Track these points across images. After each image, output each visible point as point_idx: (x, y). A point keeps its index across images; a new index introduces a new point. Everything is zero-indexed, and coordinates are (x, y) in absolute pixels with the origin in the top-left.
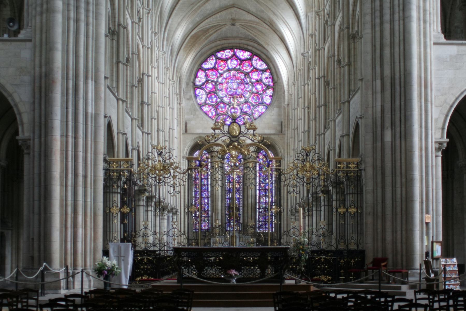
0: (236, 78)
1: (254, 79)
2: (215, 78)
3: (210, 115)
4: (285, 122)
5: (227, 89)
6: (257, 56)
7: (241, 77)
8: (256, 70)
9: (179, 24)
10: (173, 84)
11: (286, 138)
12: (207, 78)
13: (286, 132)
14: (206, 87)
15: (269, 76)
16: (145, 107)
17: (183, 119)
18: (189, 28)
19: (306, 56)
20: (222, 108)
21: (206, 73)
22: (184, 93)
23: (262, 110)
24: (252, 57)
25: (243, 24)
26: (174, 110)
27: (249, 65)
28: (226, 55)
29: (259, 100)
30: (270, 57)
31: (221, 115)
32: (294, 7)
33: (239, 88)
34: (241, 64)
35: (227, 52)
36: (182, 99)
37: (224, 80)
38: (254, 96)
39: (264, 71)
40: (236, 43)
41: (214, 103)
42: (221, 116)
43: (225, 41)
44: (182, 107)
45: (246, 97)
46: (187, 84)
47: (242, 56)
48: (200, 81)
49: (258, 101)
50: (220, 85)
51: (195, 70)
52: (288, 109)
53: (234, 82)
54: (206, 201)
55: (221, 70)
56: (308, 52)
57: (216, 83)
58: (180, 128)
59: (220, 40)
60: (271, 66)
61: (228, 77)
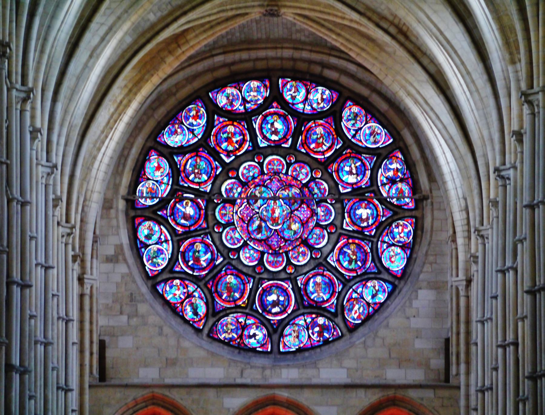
2: (206, 182)
3: (189, 315)
4: (458, 344)
5: (251, 221)
6: (356, 104)
7: (301, 177)
9: (94, 54)
10: (69, 235)
11: (462, 403)
12: (178, 184)
13: (462, 378)
15: (399, 174)
16: (16, 378)
17: (91, 332)
18: (124, 46)
19: (509, 179)
20: (230, 290)
21: (173, 165)
22: (95, 241)
23: (373, 296)
24: (337, 108)
25: (307, 13)
26: (70, 324)
29: (364, 262)
30: (402, 107)
31: (227, 315)
32: (469, 21)
33: (290, 216)
34: (301, 133)
35: (250, 90)
36: (88, 265)
37: (239, 190)
38: (347, 245)
40: (282, 59)
41: (204, 273)
42: (229, 319)
43: (244, 55)
44: (88, 291)
45: (319, 249)
47: (305, 100)
48: (152, 194)
49: (359, 263)
50: (224, 208)
51: (135, 152)
52: (468, 297)
53: (275, 198)
55: (228, 154)
56: (515, 168)
57: (208, 197)
59: (224, 53)
60: (409, 140)
61: (254, 178)
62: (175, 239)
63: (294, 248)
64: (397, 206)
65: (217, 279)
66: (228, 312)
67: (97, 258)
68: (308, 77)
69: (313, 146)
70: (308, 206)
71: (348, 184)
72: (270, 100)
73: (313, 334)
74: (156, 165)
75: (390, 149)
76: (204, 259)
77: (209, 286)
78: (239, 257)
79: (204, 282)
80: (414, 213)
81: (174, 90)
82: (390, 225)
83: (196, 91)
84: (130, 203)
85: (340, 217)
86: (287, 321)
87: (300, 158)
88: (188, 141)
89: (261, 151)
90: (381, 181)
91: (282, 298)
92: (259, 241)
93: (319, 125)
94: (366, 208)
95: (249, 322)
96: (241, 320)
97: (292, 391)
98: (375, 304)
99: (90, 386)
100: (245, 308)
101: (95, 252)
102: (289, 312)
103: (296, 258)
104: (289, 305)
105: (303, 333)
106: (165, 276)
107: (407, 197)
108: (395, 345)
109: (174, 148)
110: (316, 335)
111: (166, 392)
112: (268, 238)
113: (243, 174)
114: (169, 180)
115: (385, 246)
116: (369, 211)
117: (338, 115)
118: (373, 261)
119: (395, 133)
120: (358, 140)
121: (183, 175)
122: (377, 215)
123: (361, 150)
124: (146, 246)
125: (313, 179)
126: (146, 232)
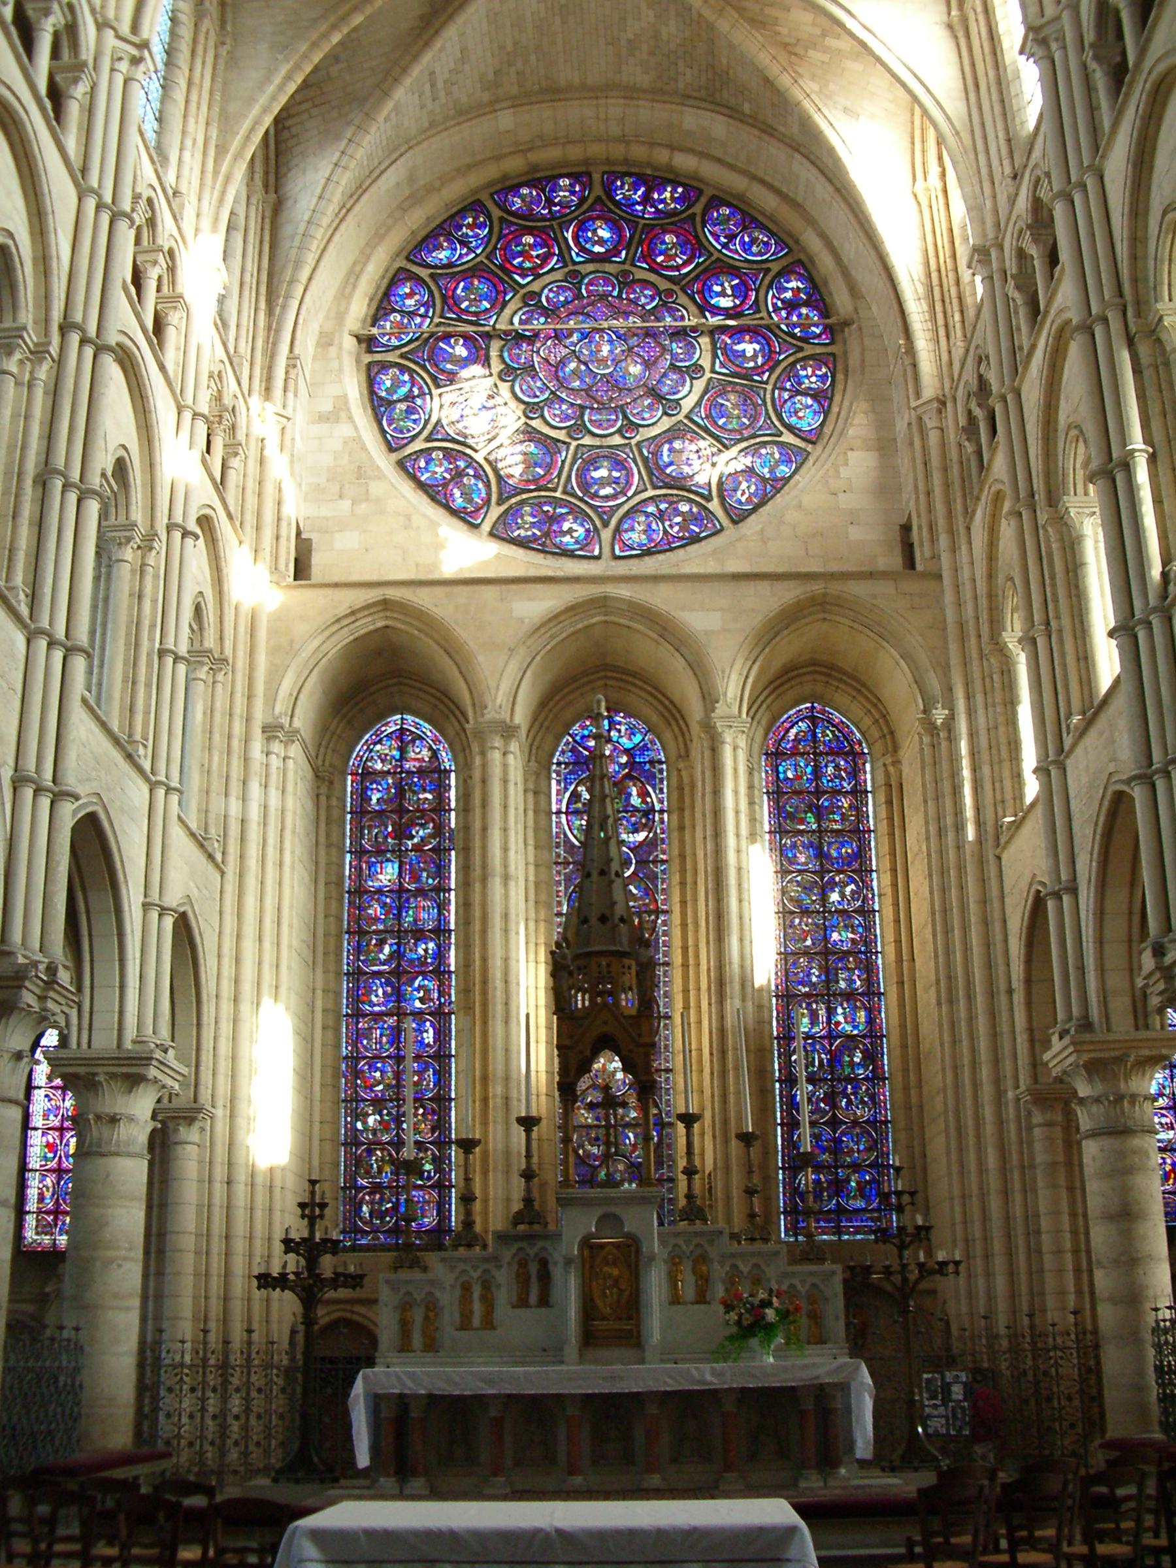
1: (716, 310)
3: (459, 502)
5: (563, 363)
6: (729, 205)
7: (643, 300)
11: (949, 597)
24: (698, 209)
27: (687, 242)
28: (550, 203)
29: (754, 418)
34: (640, 243)
38: (722, 393)
45: (677, 401)
46: (326, 341)
47: (646, 200)
48: (401, 328)
49: (745, 420)
50: (519, 347)
54: (429, 1037)
61: (567, 302)
63: (635, 400)
64: (800, 339)
66: (524, 496)
68: (649, 172)
69: (660, 259)
71: (718, 308)
72: (590, 201)
74: (407, 290)
75: (784, 262)
78: (542, 416)
80: (828, 349)
81: (437, 184)
83: (475, 192)
84: (364, 346)
86: (626, 507)
87: (640, 275)
88: (461, 256)
89: (577, 268)
90: (774, 305)
91: (616, 474)
93: (670, 232)
95: (559, 510)
96: (546, 508)
97: (637, 587)
98: (776, 480)
100: (554, 490)
101: (291, 383)
102: (630, 494)
104: (629, 484)
105: (654, 526)
107: (817, 326)
108: (814, 535)
109: (436, 267)
110: (676, 528)
112: (590, 388)
113: (547, 298)
114: (427, 311)
115: (786, 395)
116: (757, 347)
117: (698, 219)
119: (790, 242)
121: (451, 301)
124: (390, 403)
126: (388, 383)
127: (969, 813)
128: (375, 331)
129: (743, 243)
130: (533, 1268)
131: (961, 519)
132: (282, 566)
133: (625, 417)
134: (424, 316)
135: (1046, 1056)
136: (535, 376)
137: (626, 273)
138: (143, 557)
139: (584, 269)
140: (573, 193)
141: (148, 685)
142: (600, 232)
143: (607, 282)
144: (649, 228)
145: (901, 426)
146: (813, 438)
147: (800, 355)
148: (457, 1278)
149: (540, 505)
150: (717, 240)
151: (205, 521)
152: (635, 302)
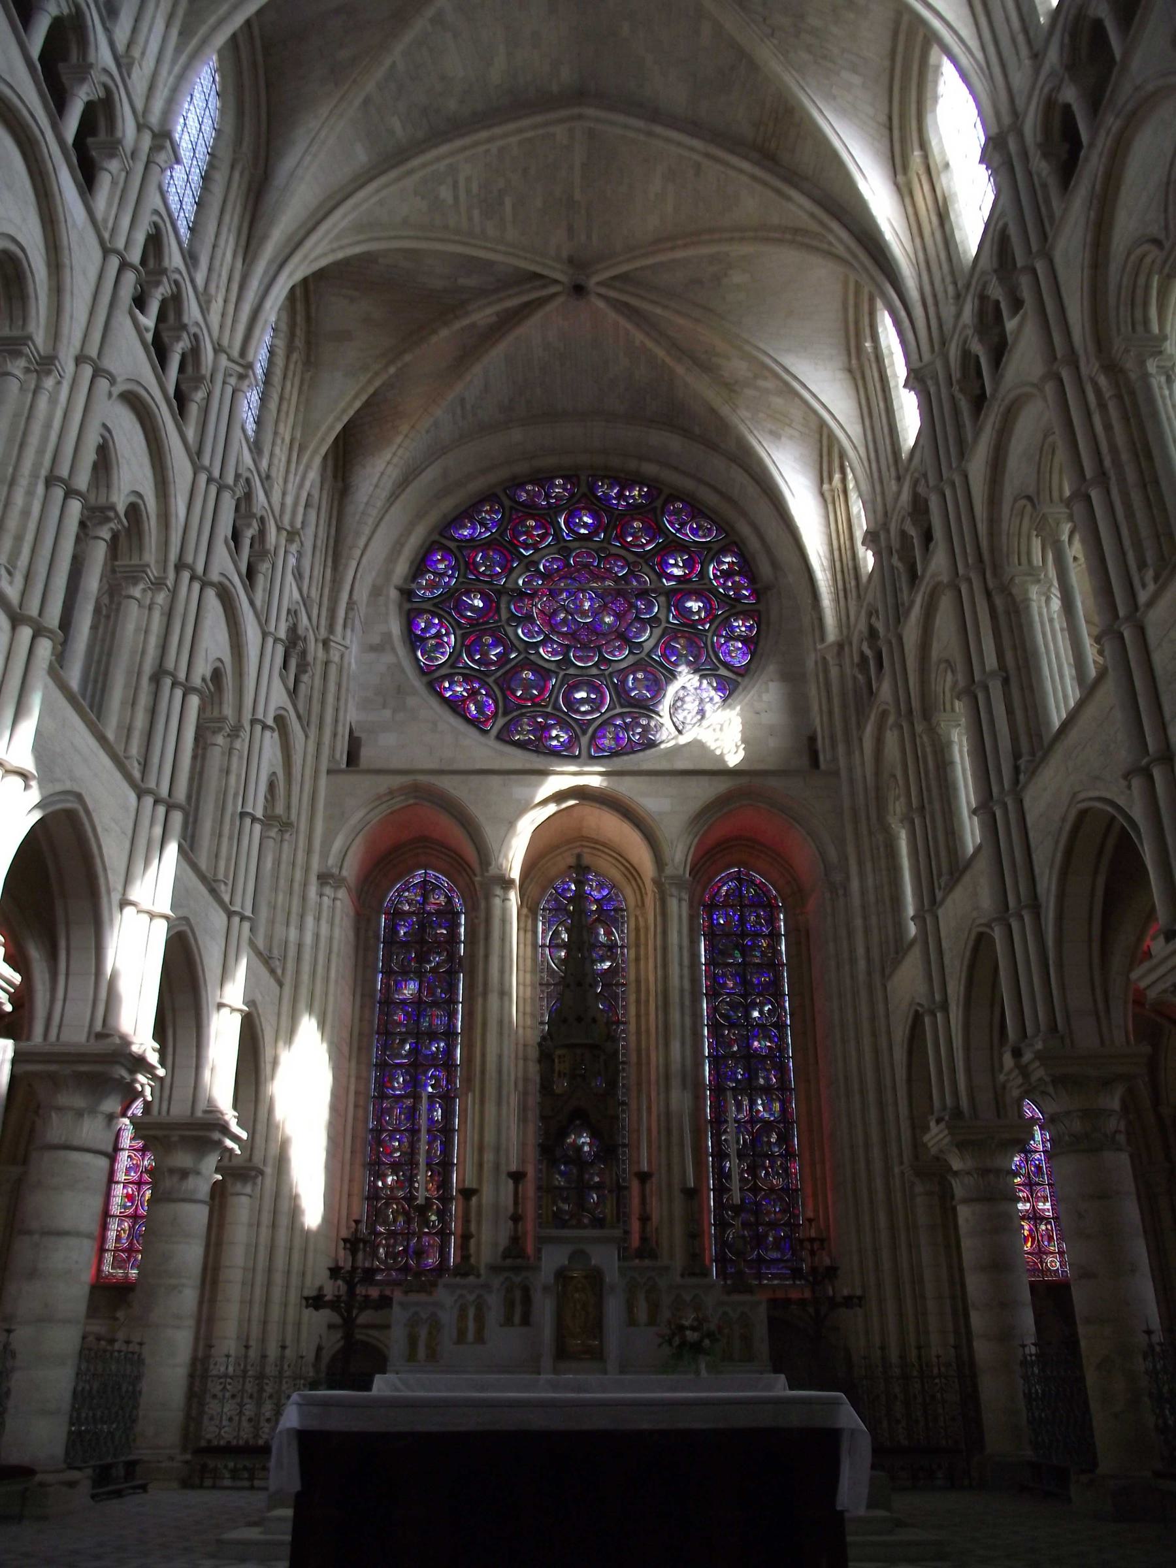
0: (592, 572)
1: (670, 577)
5: (555, 613)
6: (682, 501)
8: (678, 547)
11: (845, 789)
14: (460, 607)
20: (527, 684)
24: (658, 503)
31: (523, 715)
34: (615, 527)
38: (675, 638)
39: (713, 553)
46: (376, 592)
47: (620, 495)
48: (432, 586)
50: (522, 601)
53: (583, 591)
57: (500, 592)
58: (319, 745)
60: (745, 530)
61: (558, 569)
62: (459, 632)
65: (510, 675)
66: (524, 711)
67: (353, 630)
68: (622, 475)
69: (629, 539)
70: (626, 600)
72: (578, 496)
73: (633, 735)
76: (493, 654)
77: (500, 683)
79: (493, 678)
82: (728, 618)
85: (664, 611)
87: (614, 551)
91: (593, 696)
92: (564, 635)
94: (696, 601)
99: (329, 772)
101: (349, 622)
103: (611, 653)
104: (602, 702)
106: (444, 671)
109: (462, 541)
110: (637, 737)
111: (433, 780)
113: (545, 567)
115: (722, 641)
116: (701, 605)
118: (708, 655)
120: (683, 534)
122: (711, 608)
123: (687, 544)
124: (423, 640)
125: (631, 572)
126: (423, 625)
127: (861, 951)
128: (414, 586)
129: (691, 529)
130: (518, 1294)
131: (855, 732)
132: (338, 756)
133: (601, 655)
134: (451, 577)
135: (926, 1138)
136: (533, 623)
137: (603, 549)
138: (231, 743)
139: (571, 545)
140: (565, 489)
141: (231, 838)
142: (586, 519)
143: (589, 555)
144: (622, 515)
145: (810, 664)
146: (743, 672)
147: (733, 611)
148: (456, 1301)
149: (535, 717)
150: (673, 527)
151: (280, 720)
152: (609, 570)
